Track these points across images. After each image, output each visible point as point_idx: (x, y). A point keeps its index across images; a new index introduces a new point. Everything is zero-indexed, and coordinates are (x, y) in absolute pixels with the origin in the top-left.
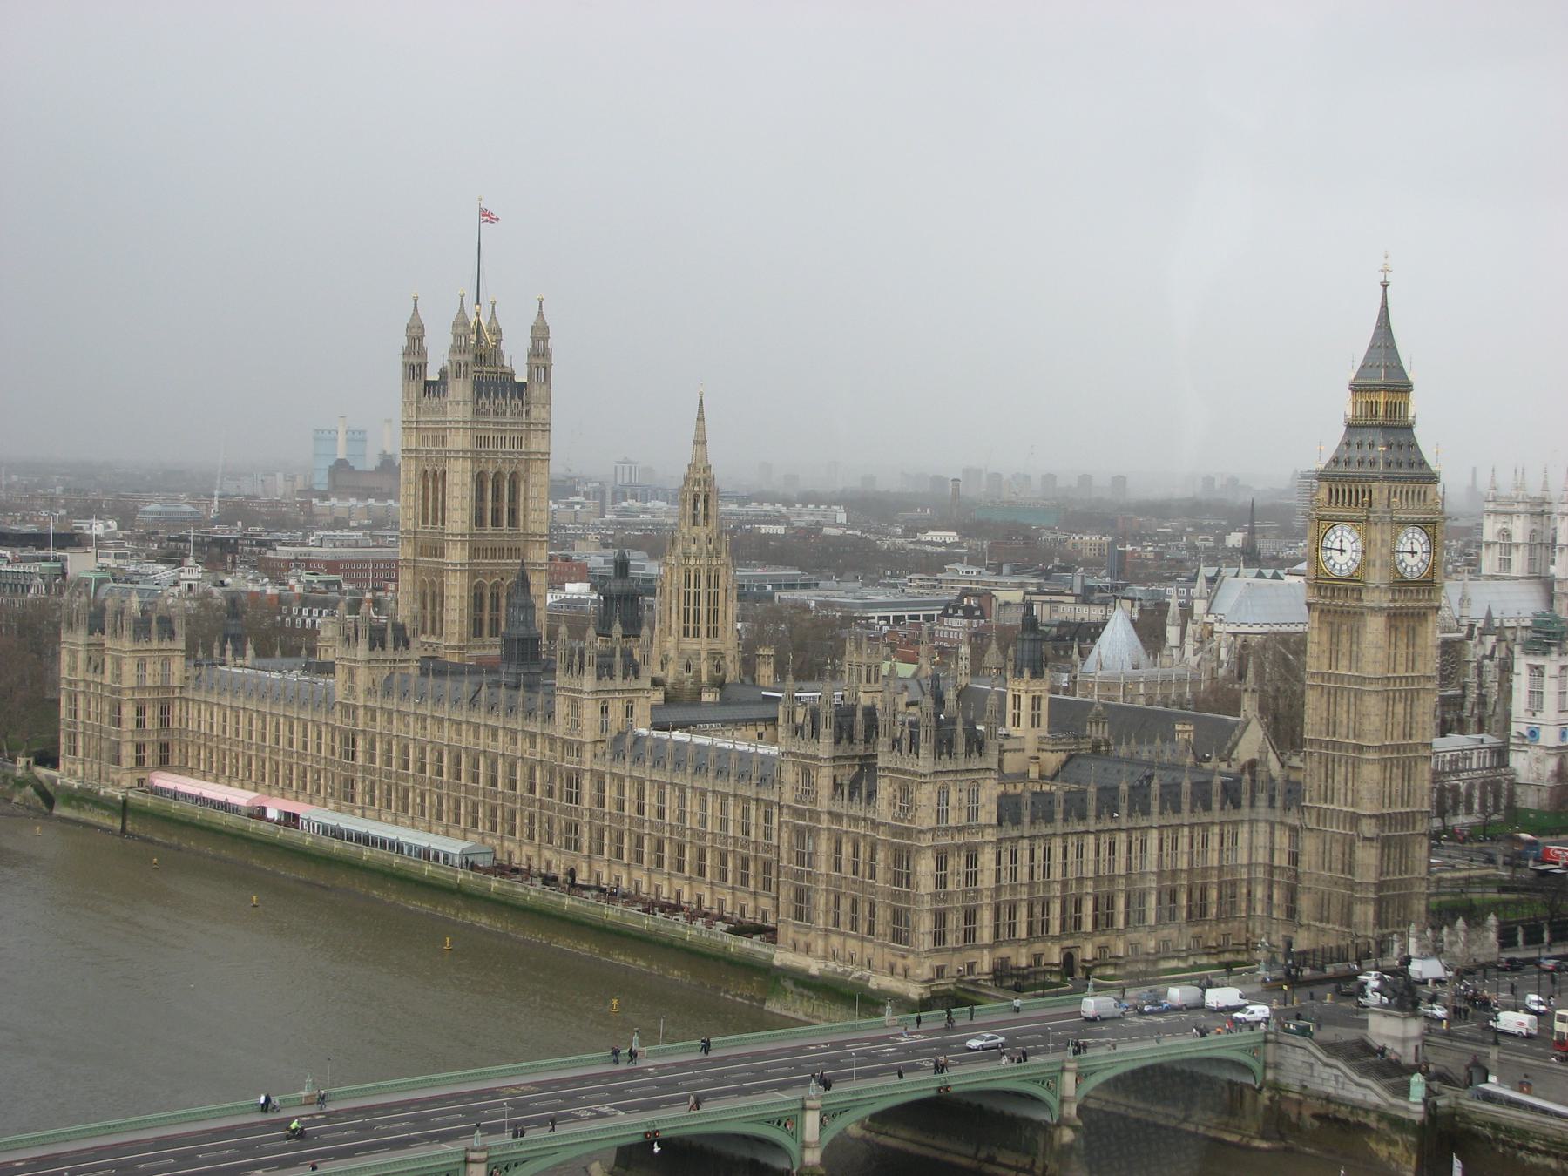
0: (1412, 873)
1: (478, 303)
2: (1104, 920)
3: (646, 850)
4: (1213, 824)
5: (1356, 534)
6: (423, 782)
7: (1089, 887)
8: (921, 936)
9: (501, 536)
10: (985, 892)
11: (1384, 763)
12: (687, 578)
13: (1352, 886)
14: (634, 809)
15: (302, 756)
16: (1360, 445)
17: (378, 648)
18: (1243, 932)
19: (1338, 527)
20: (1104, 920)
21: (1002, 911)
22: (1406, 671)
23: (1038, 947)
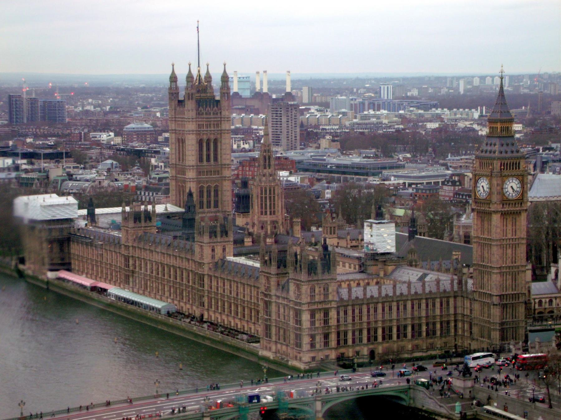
0: (518, 317)
1: (199, 66)
2: (387, 336)
3: (226, 307)
4: (436, 298)
5: (487, 181)
6: (152, 278)
7: (380, 324)
8: (304, 346)
9: (210, 165)
10: (333, 327)
11: (502, 274)
12: (262, 191)
13: (489, 322)
14: (222, 291)
15: (111, 265)
16: (491, 145)
17: (138, 222)
18: (454, 341)
19: (482, 178)
20: (387, 336)
21: (341, 334)
22: (512, 236)
23: (357, 348)
